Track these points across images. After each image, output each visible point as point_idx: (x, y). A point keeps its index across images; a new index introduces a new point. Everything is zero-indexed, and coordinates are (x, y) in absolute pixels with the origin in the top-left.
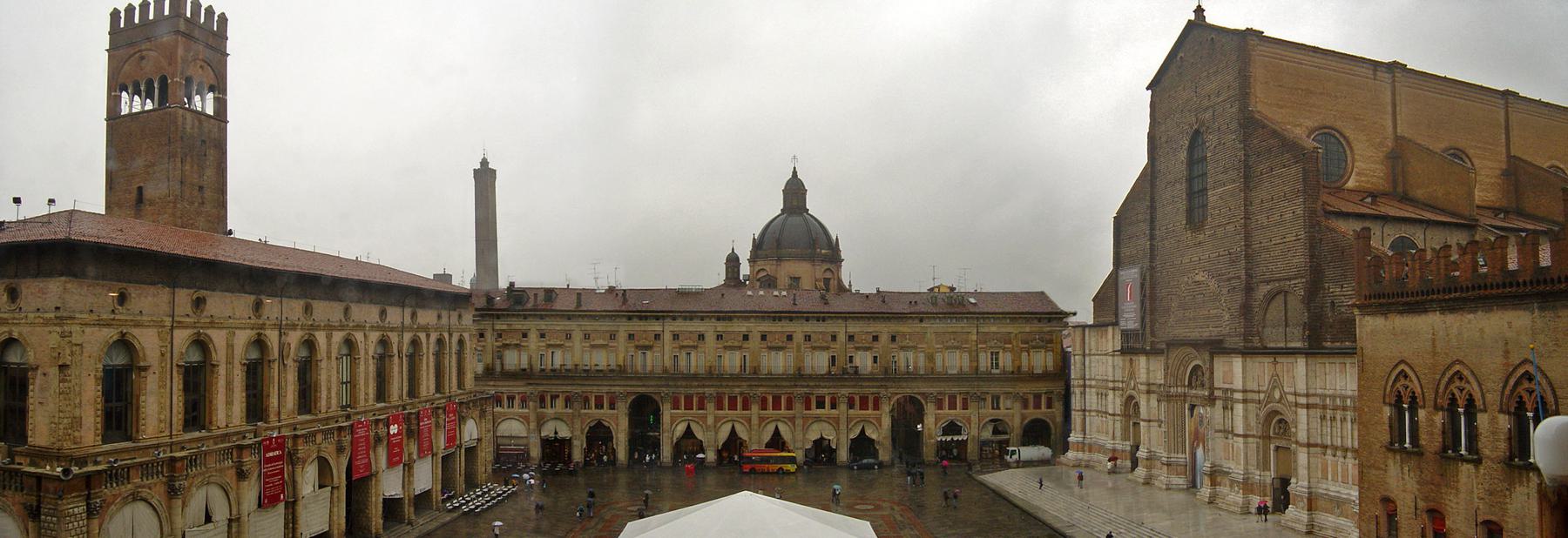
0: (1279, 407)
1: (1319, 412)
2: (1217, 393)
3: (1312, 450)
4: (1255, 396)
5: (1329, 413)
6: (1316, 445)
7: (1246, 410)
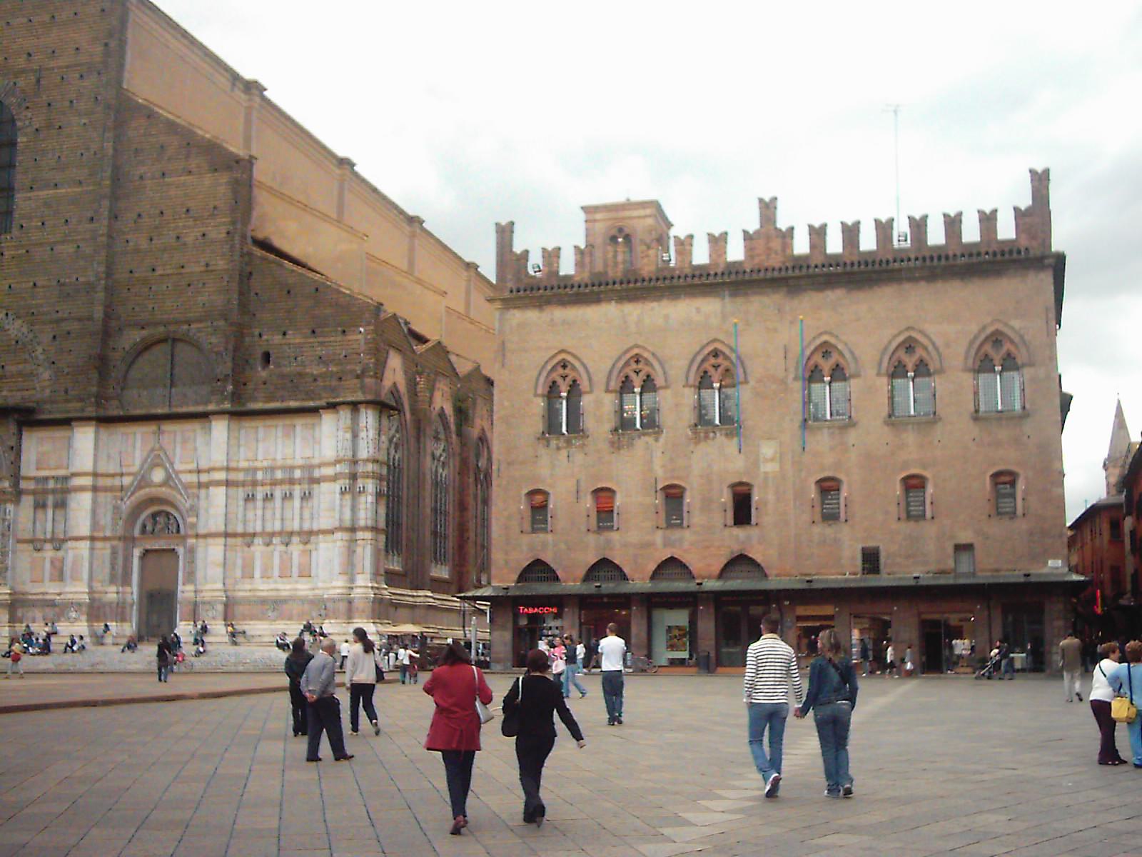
0: (164, 492)
1: (241, 493)
2: (24, 485)
3: (230, 541)
4: (117, 482)
5: (260, 492)
6: (235, 535)
7: (94, 502)
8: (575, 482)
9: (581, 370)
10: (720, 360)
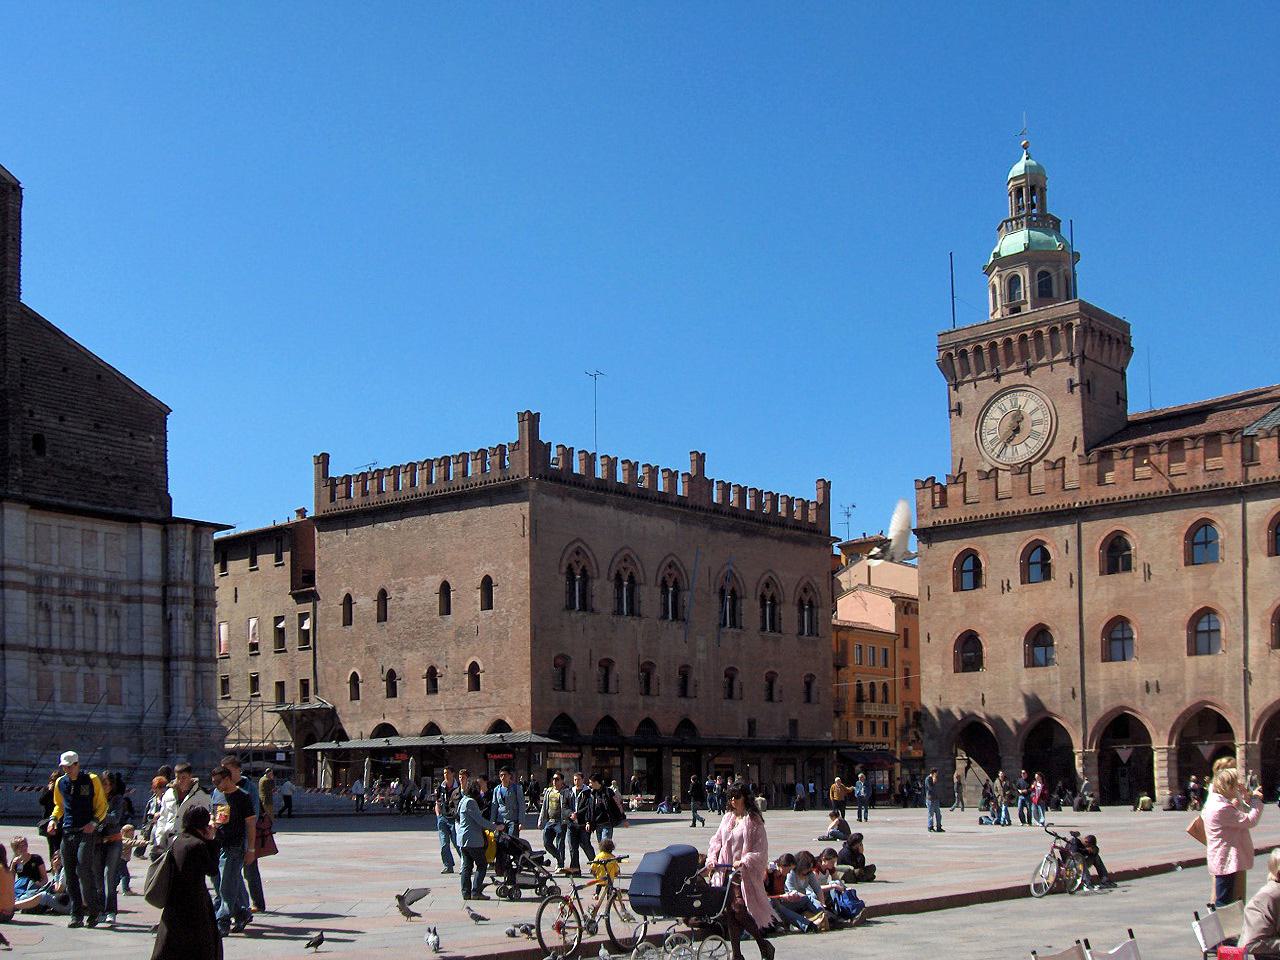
8: (588, 651)
9: (591, 558)
10: (673, 571)
